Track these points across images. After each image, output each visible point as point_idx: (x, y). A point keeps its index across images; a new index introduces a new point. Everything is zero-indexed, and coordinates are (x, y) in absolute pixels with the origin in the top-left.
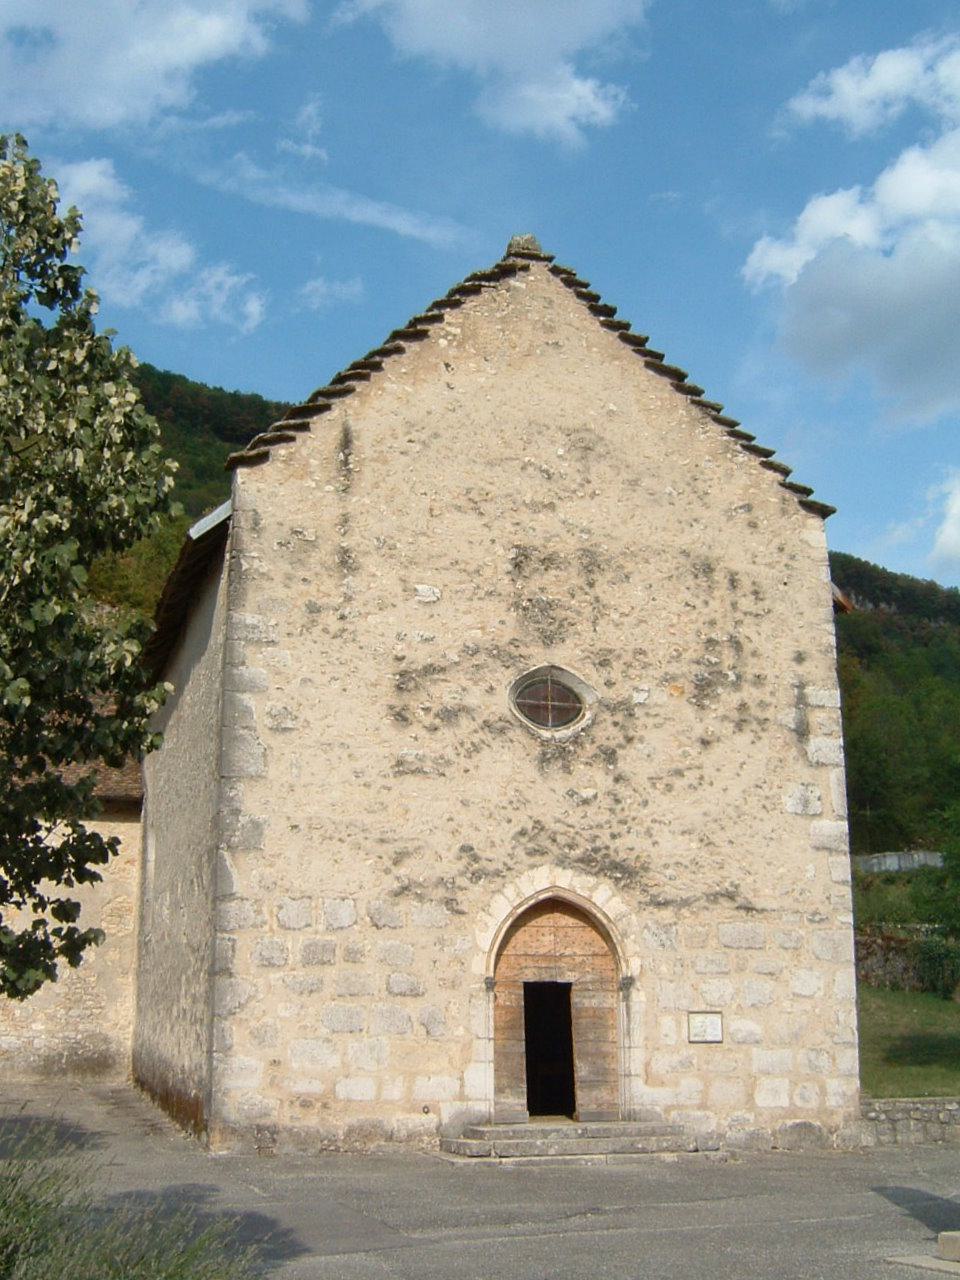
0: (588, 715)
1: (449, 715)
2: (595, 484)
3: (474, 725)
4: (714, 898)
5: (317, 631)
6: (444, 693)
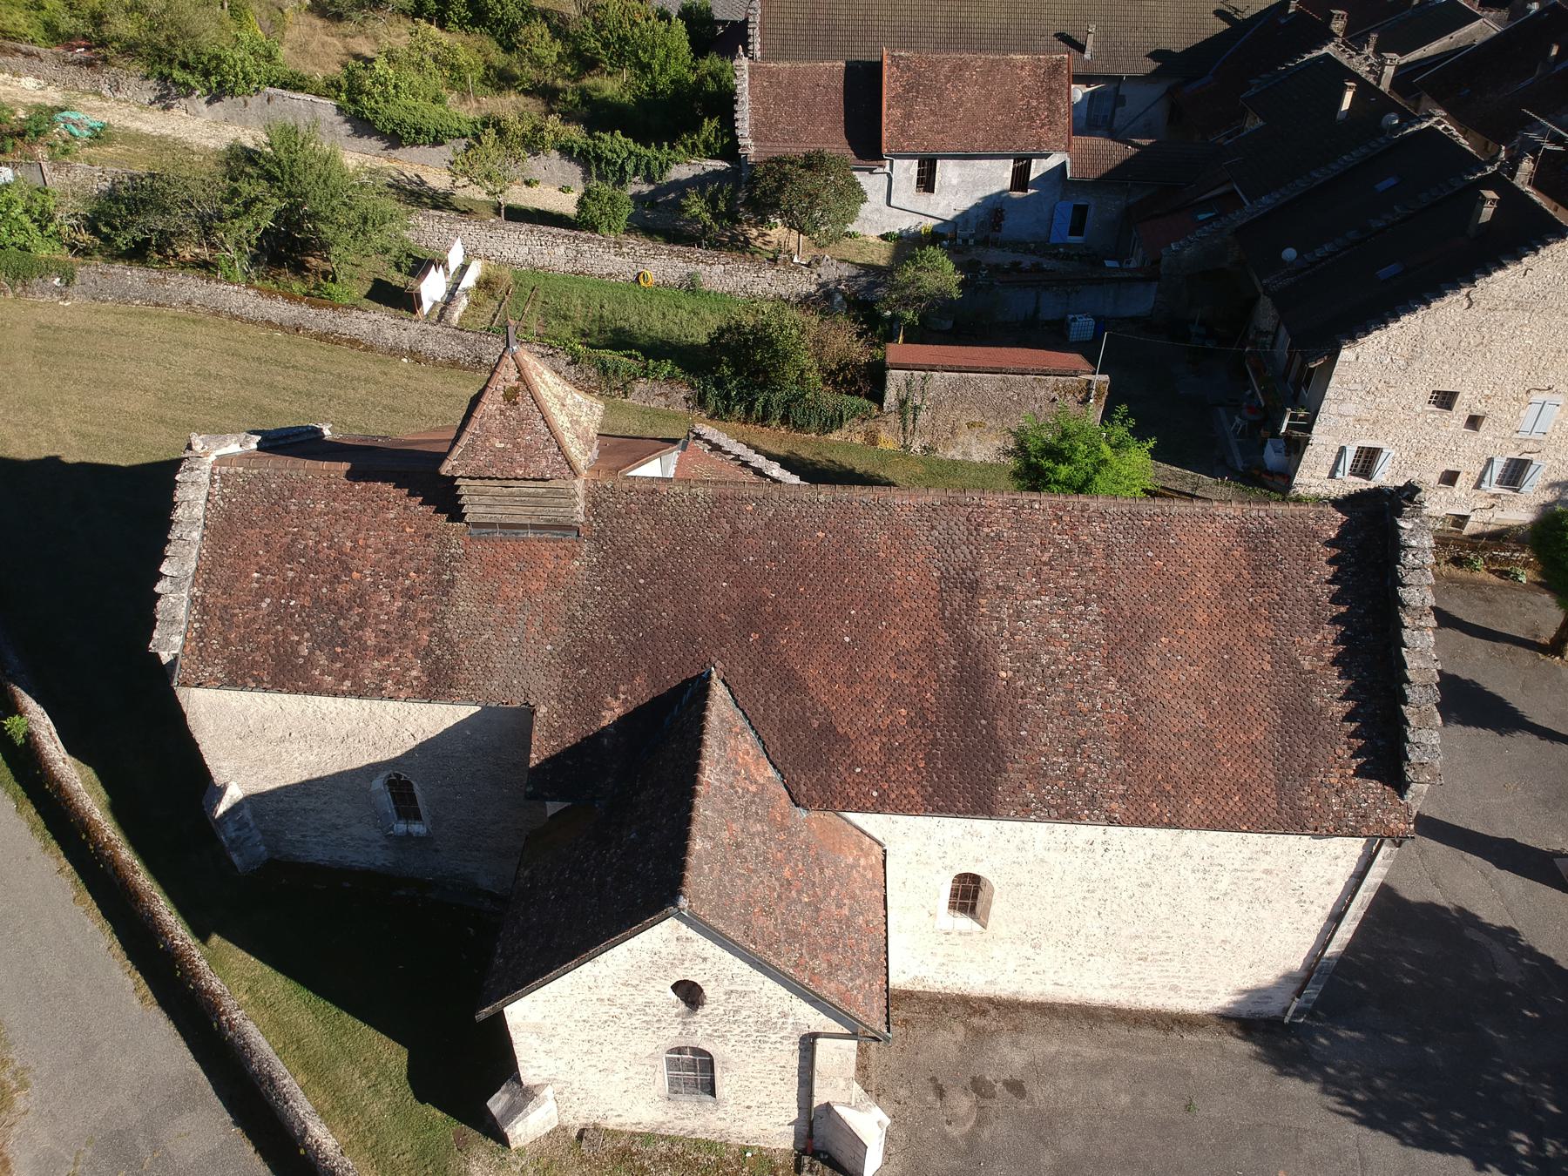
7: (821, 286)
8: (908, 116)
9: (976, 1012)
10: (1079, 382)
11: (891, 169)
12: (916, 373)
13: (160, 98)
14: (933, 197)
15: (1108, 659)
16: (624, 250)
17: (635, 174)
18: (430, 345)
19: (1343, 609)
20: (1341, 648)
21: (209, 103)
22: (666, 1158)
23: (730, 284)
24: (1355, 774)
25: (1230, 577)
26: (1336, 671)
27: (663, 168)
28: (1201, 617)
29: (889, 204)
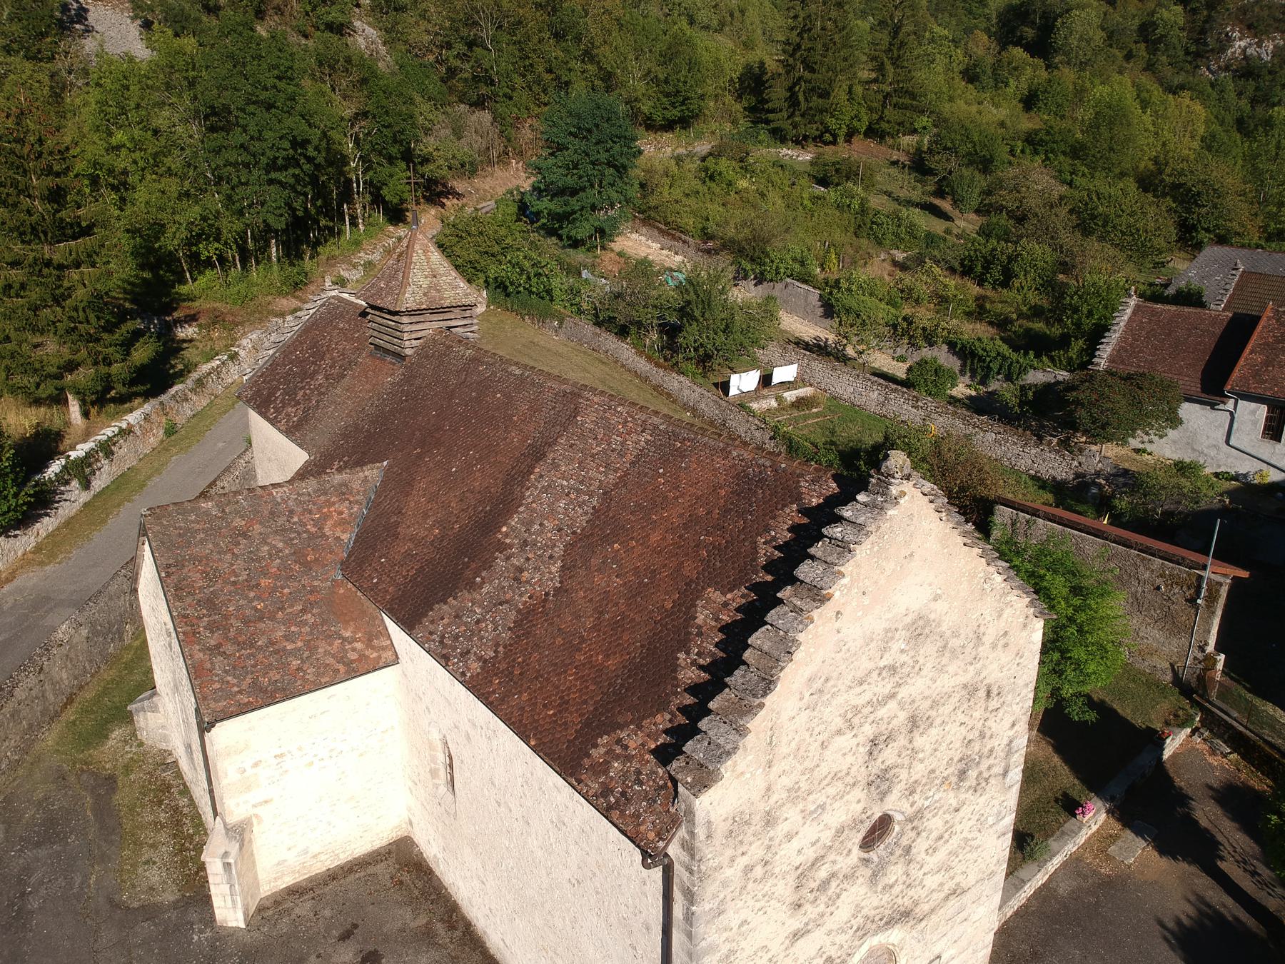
0: (897, 828)
1: (824, 885)
2: (921, 661)
3: (838, 882)
4: (947, 898)
5: (751, 885)
6: (822, 873)
7: (1077, 475)
8: (1267, 363)
9: (448, 922)
10: (1189, 575)
11: (1235, 408)
12: (1021, 514)
13: (735, 278)
14: (1279, 446)
15: (569, 547)
16: (919, 404)
17: (998, 373)
18: (703, 406)
19: (769, 578)
20: (739, 616)
21: (755, 285)
22: (176, 809)
23: (998, 452)
24: (653, 752)
25: (701, 512)
26: (720, 636)
27: (1023, 371)
28: (655, 537)
29: (1227, 442)
